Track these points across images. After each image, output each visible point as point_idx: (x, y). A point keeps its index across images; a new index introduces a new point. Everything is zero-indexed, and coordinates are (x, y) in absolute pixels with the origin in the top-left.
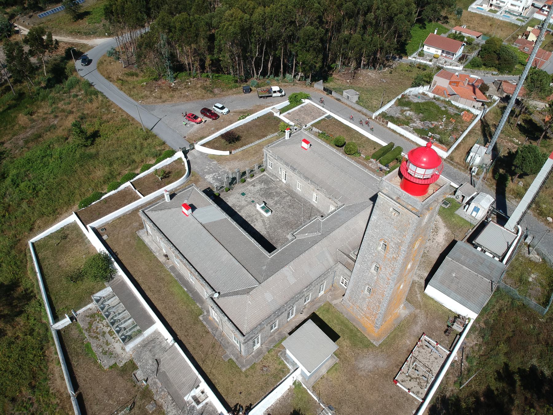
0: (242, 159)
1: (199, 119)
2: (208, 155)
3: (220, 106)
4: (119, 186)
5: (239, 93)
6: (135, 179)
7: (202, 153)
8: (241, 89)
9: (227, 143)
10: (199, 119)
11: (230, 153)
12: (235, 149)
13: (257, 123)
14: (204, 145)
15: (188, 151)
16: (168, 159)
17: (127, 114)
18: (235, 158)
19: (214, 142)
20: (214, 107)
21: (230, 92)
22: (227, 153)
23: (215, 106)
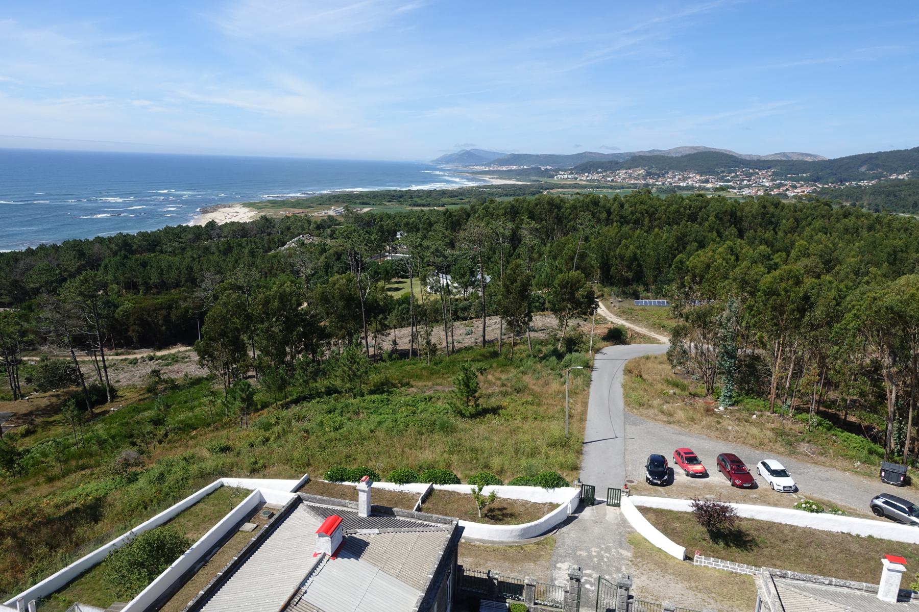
0: (708, 590)
1: (698, 468)
2: (632, 532)
3: (775, 465)
4: (408, 482)
5: (869, 475)
6: (447, 487)
7: (624, 522)
8: (875, 470)
9: (708, 537)
10: (698, 468)
11: (688, 558)
12: (706, 553)
13: (855, 547)
14: (644, 510)
15: (600, 502)
16: (539, 489)
17: (584, 412)
18: (693, 578)
19: (678, 519)
20: (760, 465)
21: (841, 463)
22: (677, 551)
23: (764, 464)
